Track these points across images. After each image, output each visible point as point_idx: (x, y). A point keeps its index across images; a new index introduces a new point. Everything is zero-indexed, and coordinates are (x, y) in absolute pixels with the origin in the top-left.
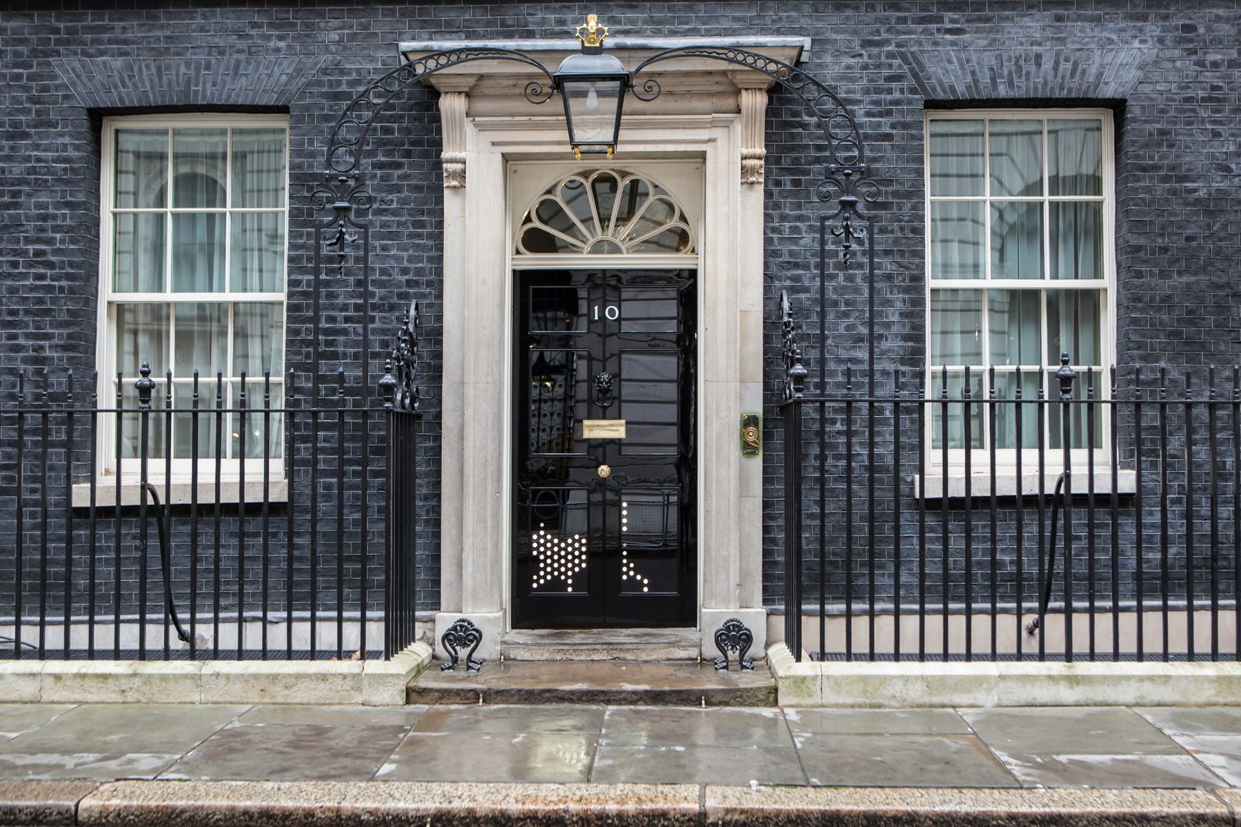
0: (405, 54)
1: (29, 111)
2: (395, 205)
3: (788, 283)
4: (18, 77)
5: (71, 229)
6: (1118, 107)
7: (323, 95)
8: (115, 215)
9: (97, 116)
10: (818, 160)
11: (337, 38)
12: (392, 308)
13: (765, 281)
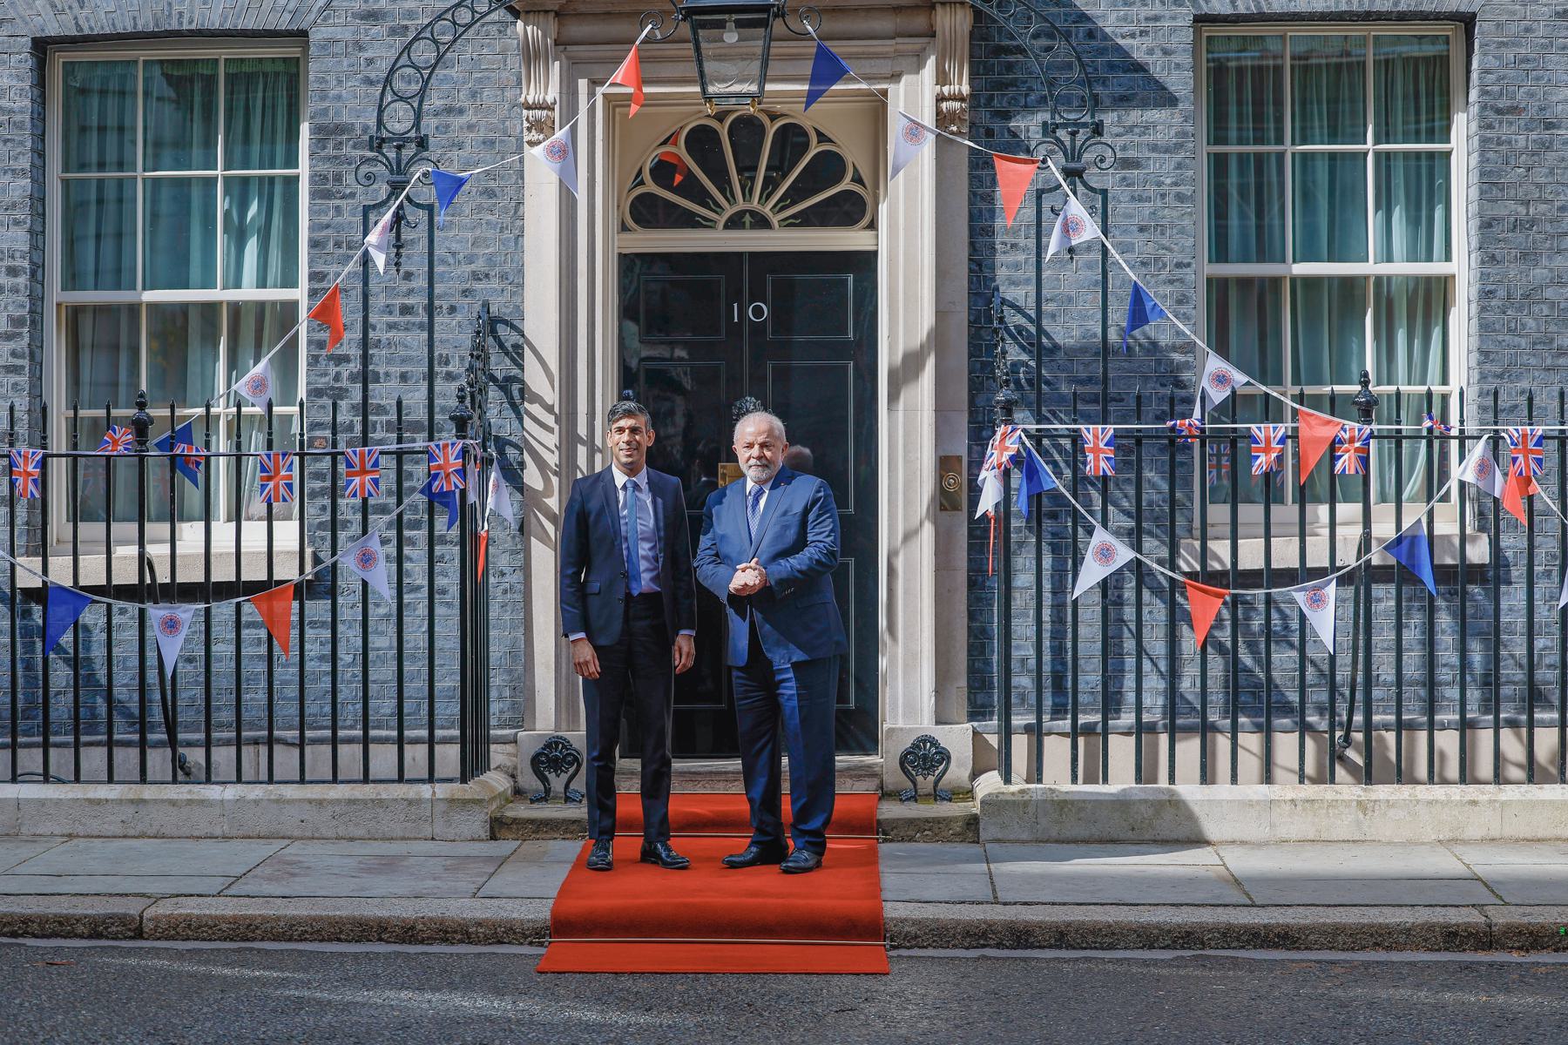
5: (14, 205)
7: (354, 16)
8: (66, 183)
9: (42, 47)
12: (452, 309)
13: (971, 270)
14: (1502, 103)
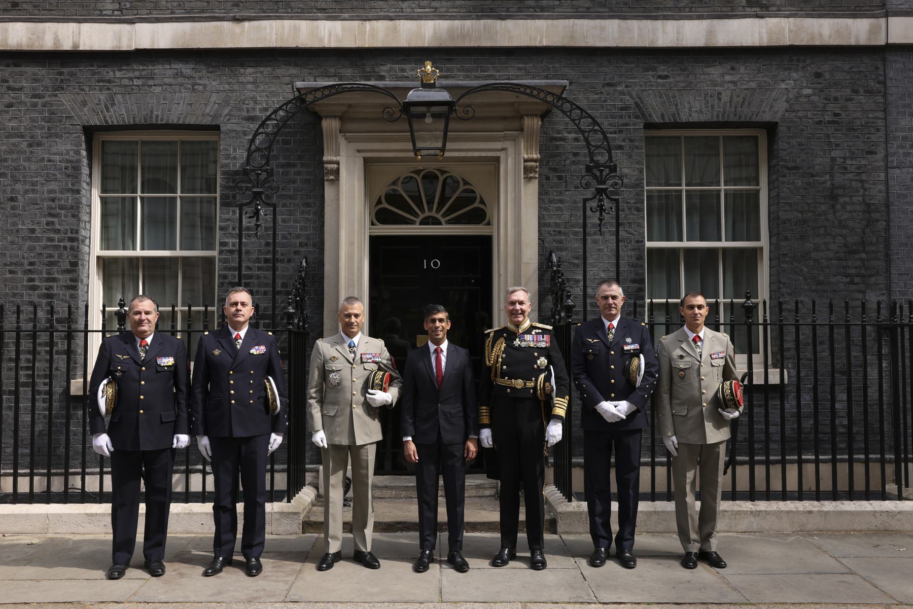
0: (298, 90)
1: (43, 128)
2: (291, 193)
3: (555, 244)
4: (35, 105)
5: (72, 208)
6: (771, 128)
8: (101, 198)
9: (90, 132)
10: (574, 163)
11: (252, 80)
12: (289, 261)
14: (790, 165)
